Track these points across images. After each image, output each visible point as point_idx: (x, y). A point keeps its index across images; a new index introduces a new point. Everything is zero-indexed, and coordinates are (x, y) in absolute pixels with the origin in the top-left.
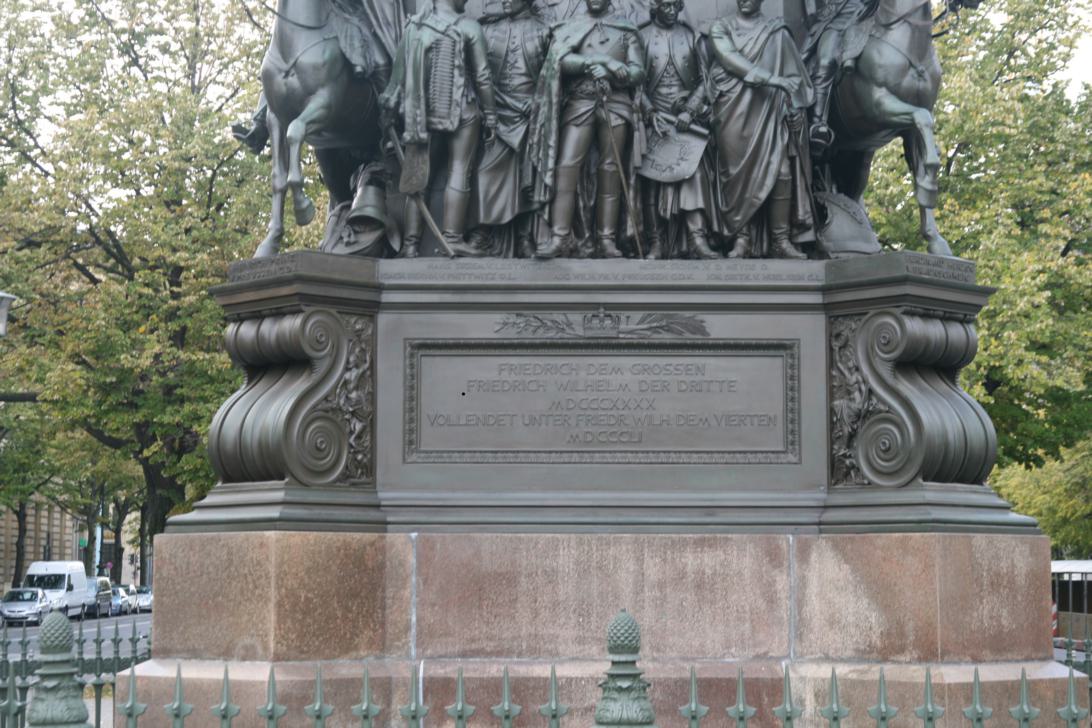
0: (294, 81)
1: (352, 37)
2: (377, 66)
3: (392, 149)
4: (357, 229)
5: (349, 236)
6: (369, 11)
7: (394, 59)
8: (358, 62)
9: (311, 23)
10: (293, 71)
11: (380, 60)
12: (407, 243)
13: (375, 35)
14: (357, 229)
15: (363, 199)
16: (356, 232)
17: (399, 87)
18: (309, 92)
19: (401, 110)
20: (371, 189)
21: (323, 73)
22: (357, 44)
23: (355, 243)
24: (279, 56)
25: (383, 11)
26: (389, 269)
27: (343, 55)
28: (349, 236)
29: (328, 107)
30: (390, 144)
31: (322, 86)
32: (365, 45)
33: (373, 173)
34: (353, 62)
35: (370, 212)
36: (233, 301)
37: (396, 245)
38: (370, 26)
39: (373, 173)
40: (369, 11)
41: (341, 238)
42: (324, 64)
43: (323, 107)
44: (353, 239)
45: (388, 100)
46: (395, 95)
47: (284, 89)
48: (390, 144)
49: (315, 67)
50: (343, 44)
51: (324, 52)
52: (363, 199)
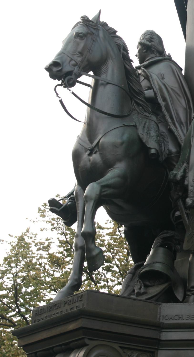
0: (96, 157)
1: (149, 129)
2: (170, 153)
3: (180, 217)
4: (148, 283)
5: (140, 289)
6: (166, 113)
7: (182, 144)
8: (152, 144)
9: (114, 113)
10: (96, 149)
11: (173, 148)
12: (189, 293)
13: (170, 131)
14: (148, 283)
15: (153, 257)
16: (146, 286)
17: (185, 165)
18: (109, 165)
19: (186, 183)
20: (161, 250)
21: (120, 151)
22: (153, 133)
23: (144, 293)
24: (87, 139)
25: (178, 114)
26: (170, 311)
27: (140, 140)
28: (140, 289)
29: (124, 177)
30: (177, 213)
31: (120, 160)
32: (160, 135)
33: (164, 239)
34: (149, 146)
35: (158, 267)
36: (37, 339)
37: (180, 296)
38: (166, 124)
39: (164, 239)
40: (166, 113)
41: (134, 291)
42: (122, 143)
43: (119, 176)
44: (142, 290)
45: (175, 175)
46: (182, 170)
47: (88, 164)
48: (177, 213)
49: (115, 146)
50: (140, 132)
51: (123, 134)
52: (153, 257)
